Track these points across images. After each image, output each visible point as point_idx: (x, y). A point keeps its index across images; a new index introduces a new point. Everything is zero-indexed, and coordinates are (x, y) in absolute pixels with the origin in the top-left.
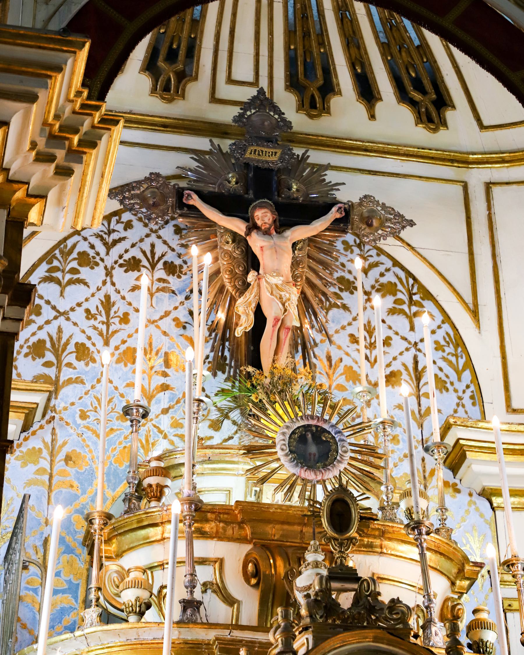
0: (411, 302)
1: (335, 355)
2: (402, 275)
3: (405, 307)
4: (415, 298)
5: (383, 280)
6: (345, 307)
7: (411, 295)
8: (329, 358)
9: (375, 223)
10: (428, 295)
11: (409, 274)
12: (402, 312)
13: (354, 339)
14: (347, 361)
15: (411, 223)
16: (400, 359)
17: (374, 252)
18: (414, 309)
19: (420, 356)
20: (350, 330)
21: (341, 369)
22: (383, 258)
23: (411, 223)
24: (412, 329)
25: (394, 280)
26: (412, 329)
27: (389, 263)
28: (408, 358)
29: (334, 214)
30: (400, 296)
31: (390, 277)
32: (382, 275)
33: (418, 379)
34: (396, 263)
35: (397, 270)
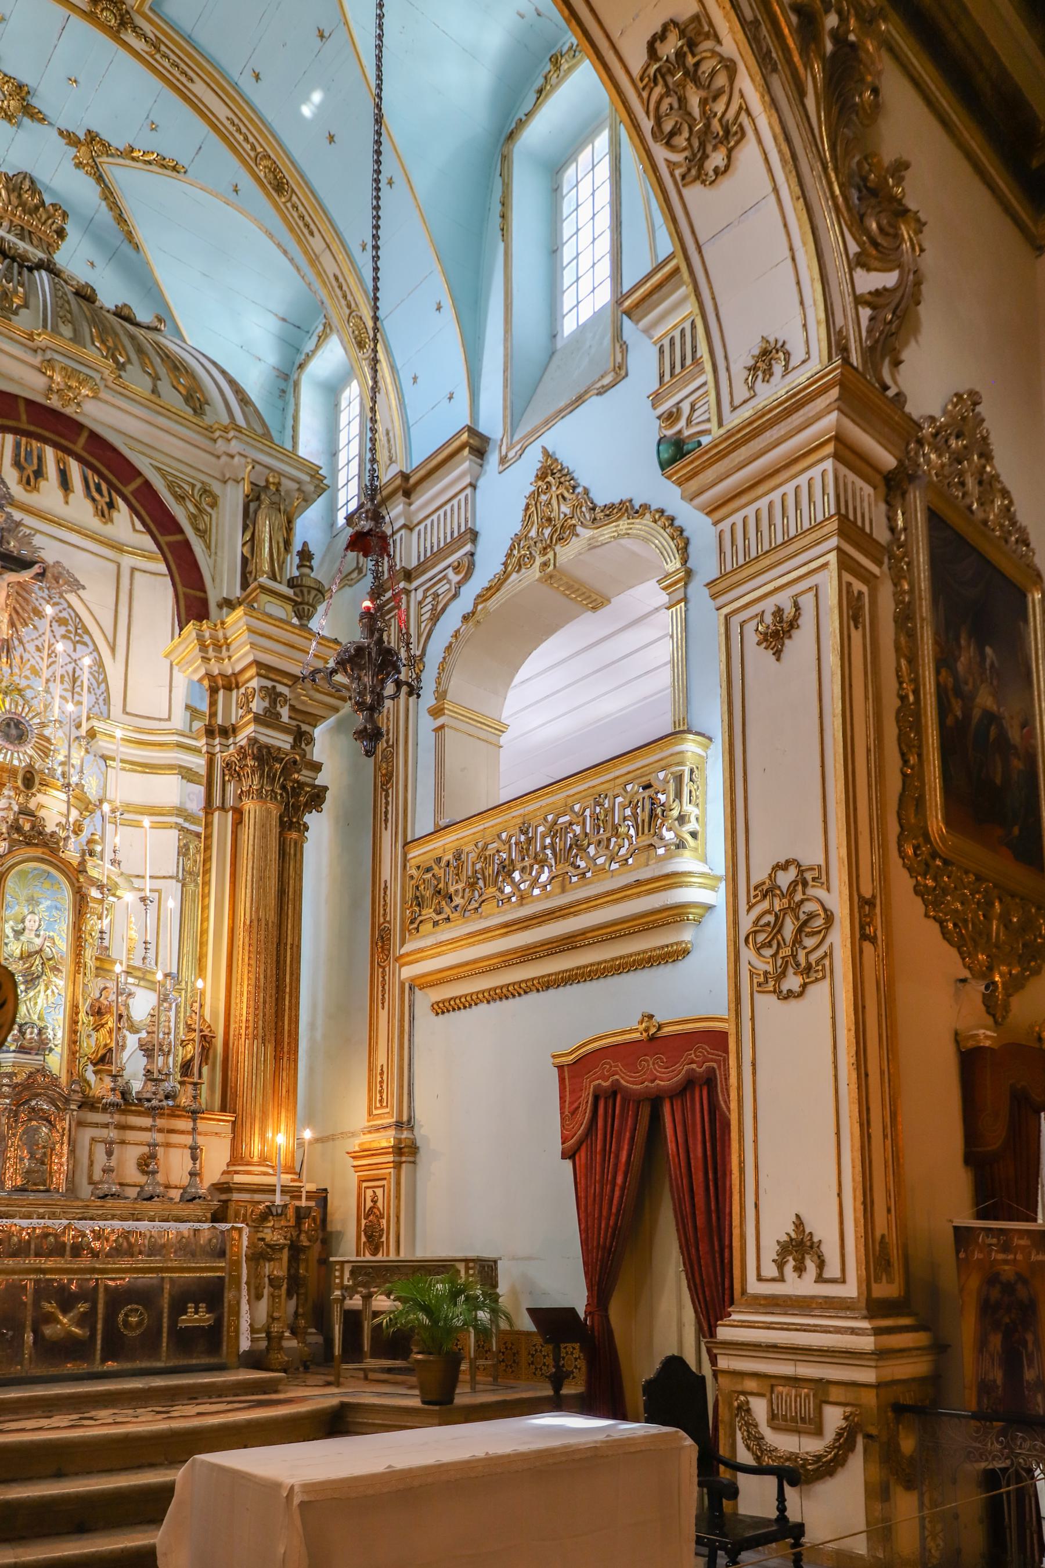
0: (76, 634)
1: (26, 656)
2: (73, 614)
3: (72, 636)
4: (79, 631)
5: (61, 615)
6: (35, 628)
7: (76, 629)
8: (22, 658)
9: (61, 582)
10: (86, 631)
11: (77, 615)
12: (69, 638)
13: (38, 649)
14: (32, 662)
15: (84, 588)
16: (66, 668)
17: (57, 596)
18: (77, 638)
19: (77, 669)
20: (37, 642)
21: (28, 665)
22: (62, 601)
23: (84, 588)
24: (75, 650)
25: (67, 616)
26: (75, 650)
27: (65, 605)
28: (70, 668)
29: (36, 569)
30: (70, 628)
31: (64, 614)
32: (60, 612)
33: (74, 682)
34: (70, 606)
35: (70, 610)
